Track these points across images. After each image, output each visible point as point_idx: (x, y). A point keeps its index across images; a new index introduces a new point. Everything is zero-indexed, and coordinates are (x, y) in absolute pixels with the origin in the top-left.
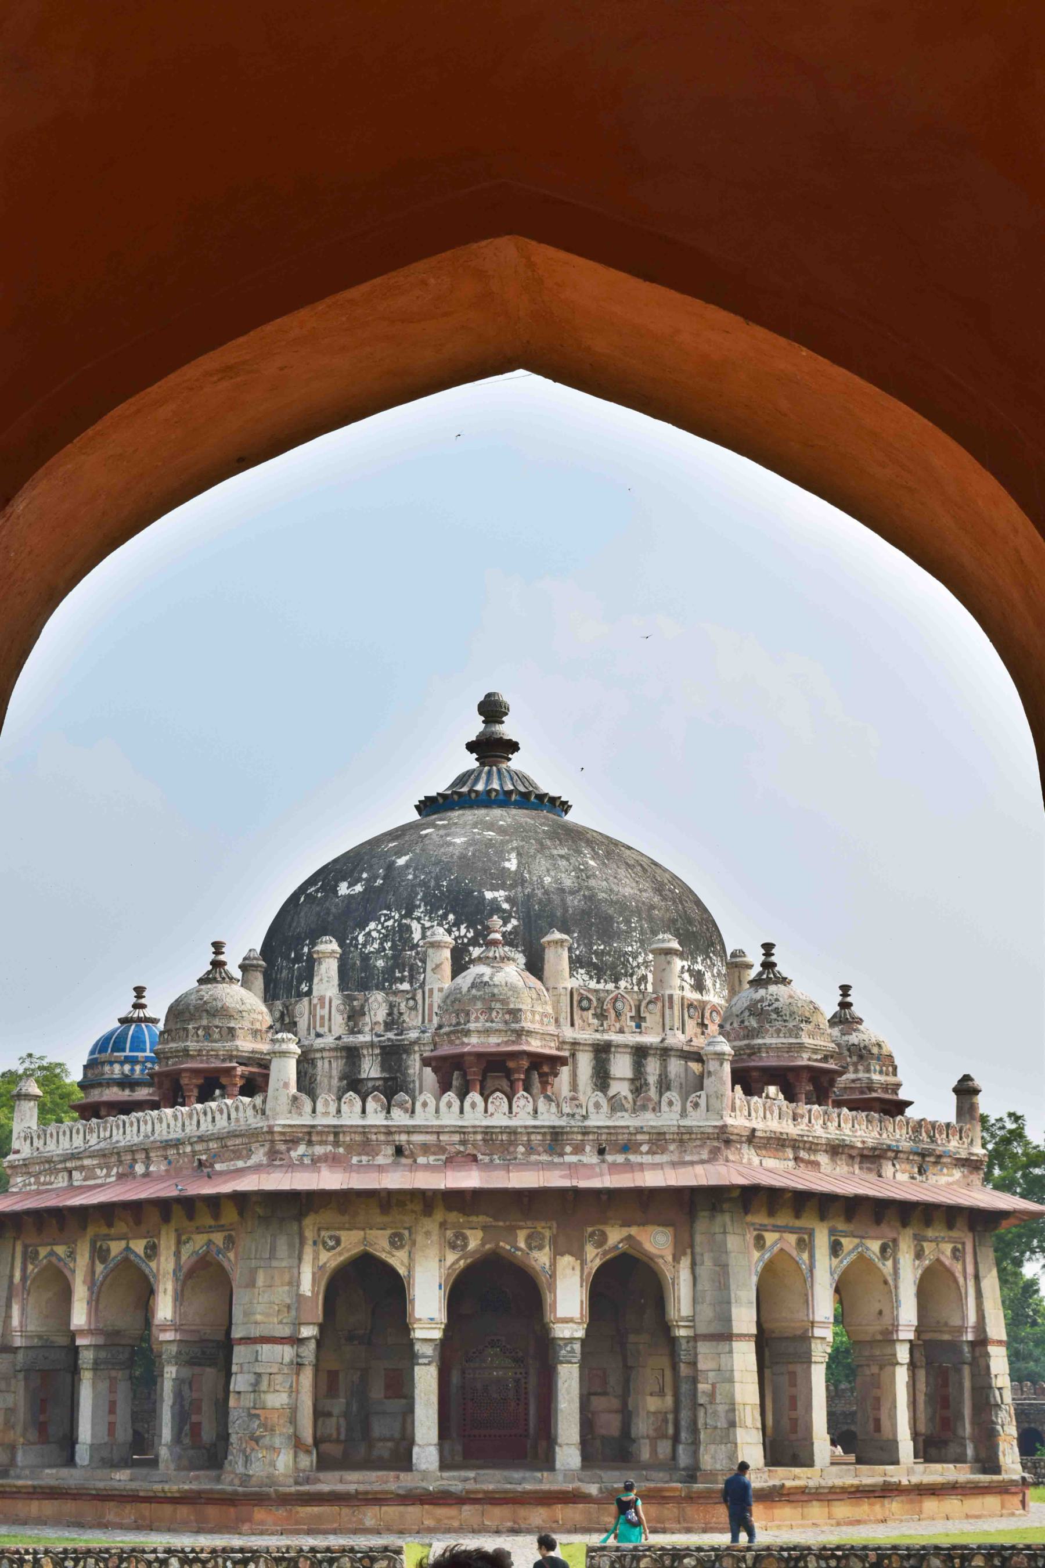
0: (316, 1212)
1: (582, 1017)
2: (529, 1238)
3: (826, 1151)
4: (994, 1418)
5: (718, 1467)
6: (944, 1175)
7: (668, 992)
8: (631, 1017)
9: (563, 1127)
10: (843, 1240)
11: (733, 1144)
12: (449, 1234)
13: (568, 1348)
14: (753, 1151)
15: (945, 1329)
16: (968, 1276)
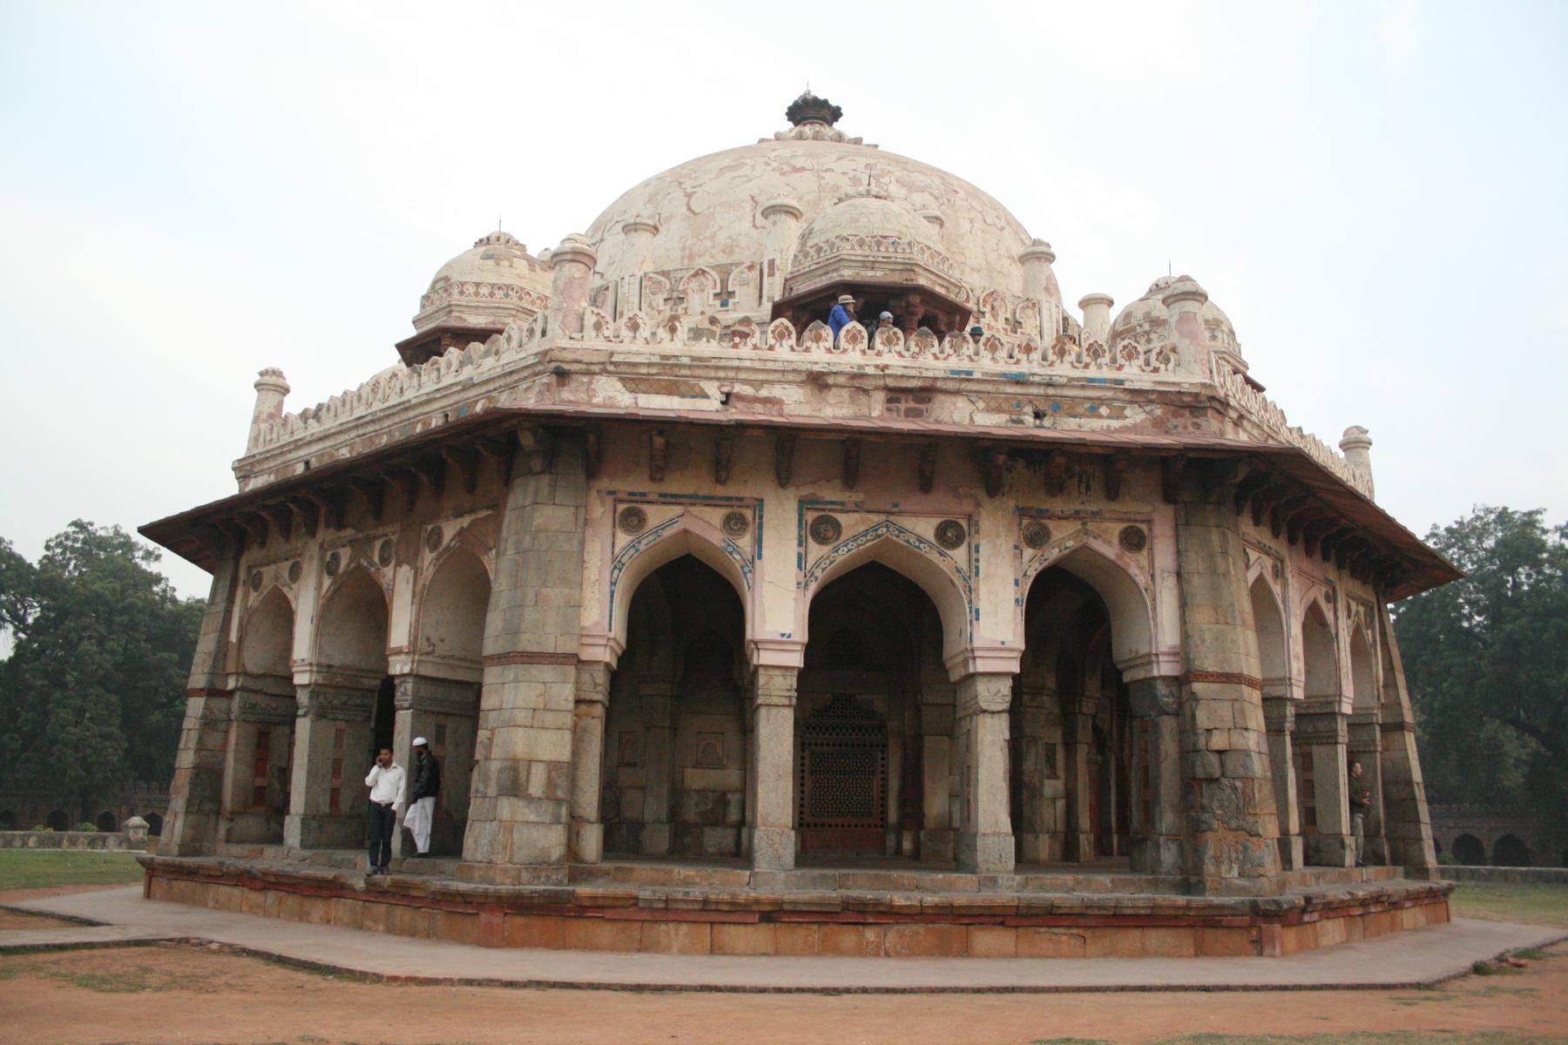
0: (249, 549)
1: (650, 305)
2: (383, 548)
3: (801, 384)
4: (1205, 801)
5: (479, 857)
6: (1100, 417)
7: (771, 257)
8: (716, 295)
9: (409, 401)
10: (842, 518)
11: (573, 377)
12: (329, 554)
13: (402, 689)
14: (619, 385)
15: (1139, 661)
16: (1157, 573)
